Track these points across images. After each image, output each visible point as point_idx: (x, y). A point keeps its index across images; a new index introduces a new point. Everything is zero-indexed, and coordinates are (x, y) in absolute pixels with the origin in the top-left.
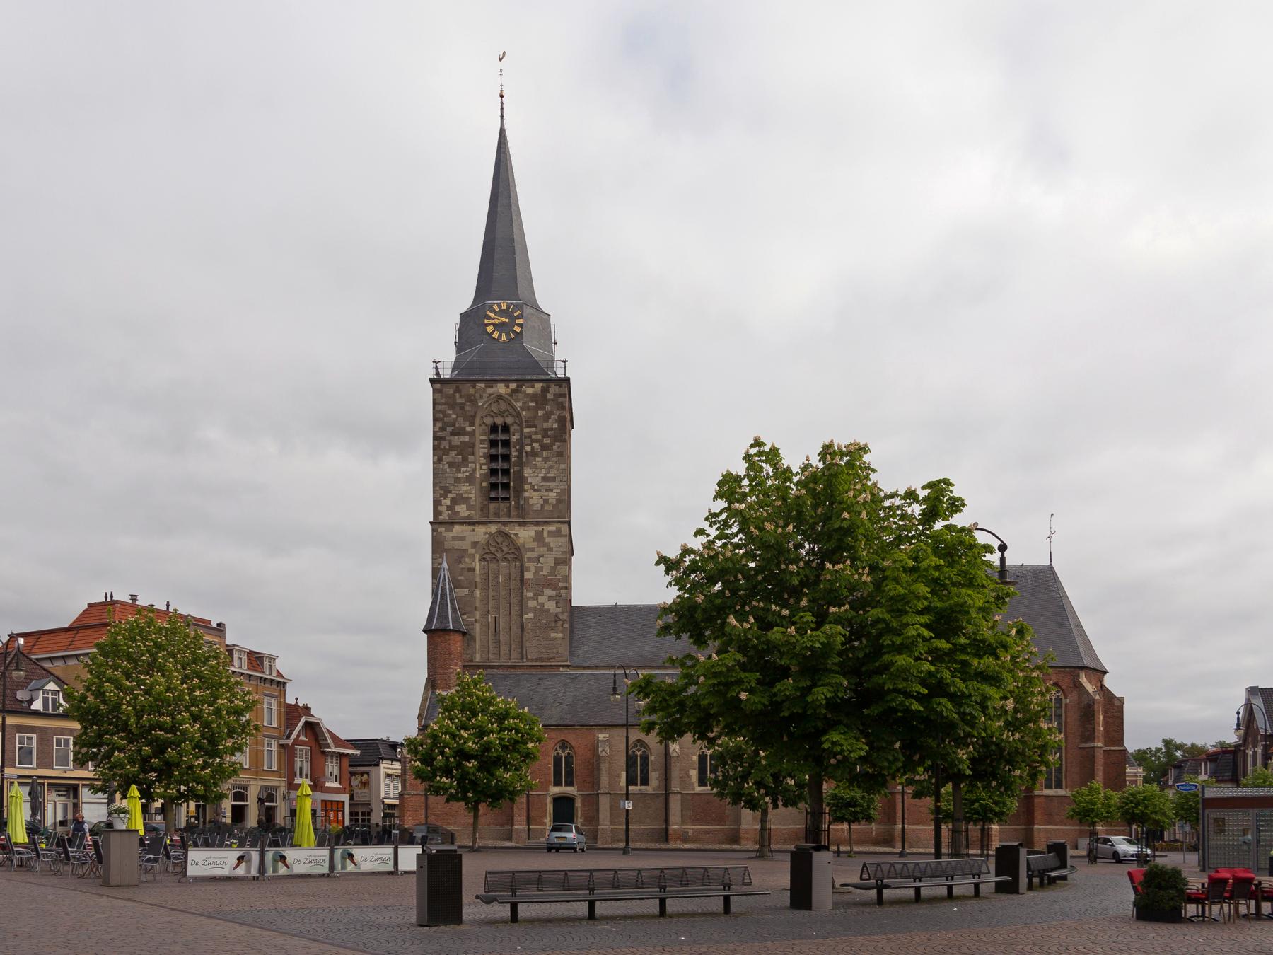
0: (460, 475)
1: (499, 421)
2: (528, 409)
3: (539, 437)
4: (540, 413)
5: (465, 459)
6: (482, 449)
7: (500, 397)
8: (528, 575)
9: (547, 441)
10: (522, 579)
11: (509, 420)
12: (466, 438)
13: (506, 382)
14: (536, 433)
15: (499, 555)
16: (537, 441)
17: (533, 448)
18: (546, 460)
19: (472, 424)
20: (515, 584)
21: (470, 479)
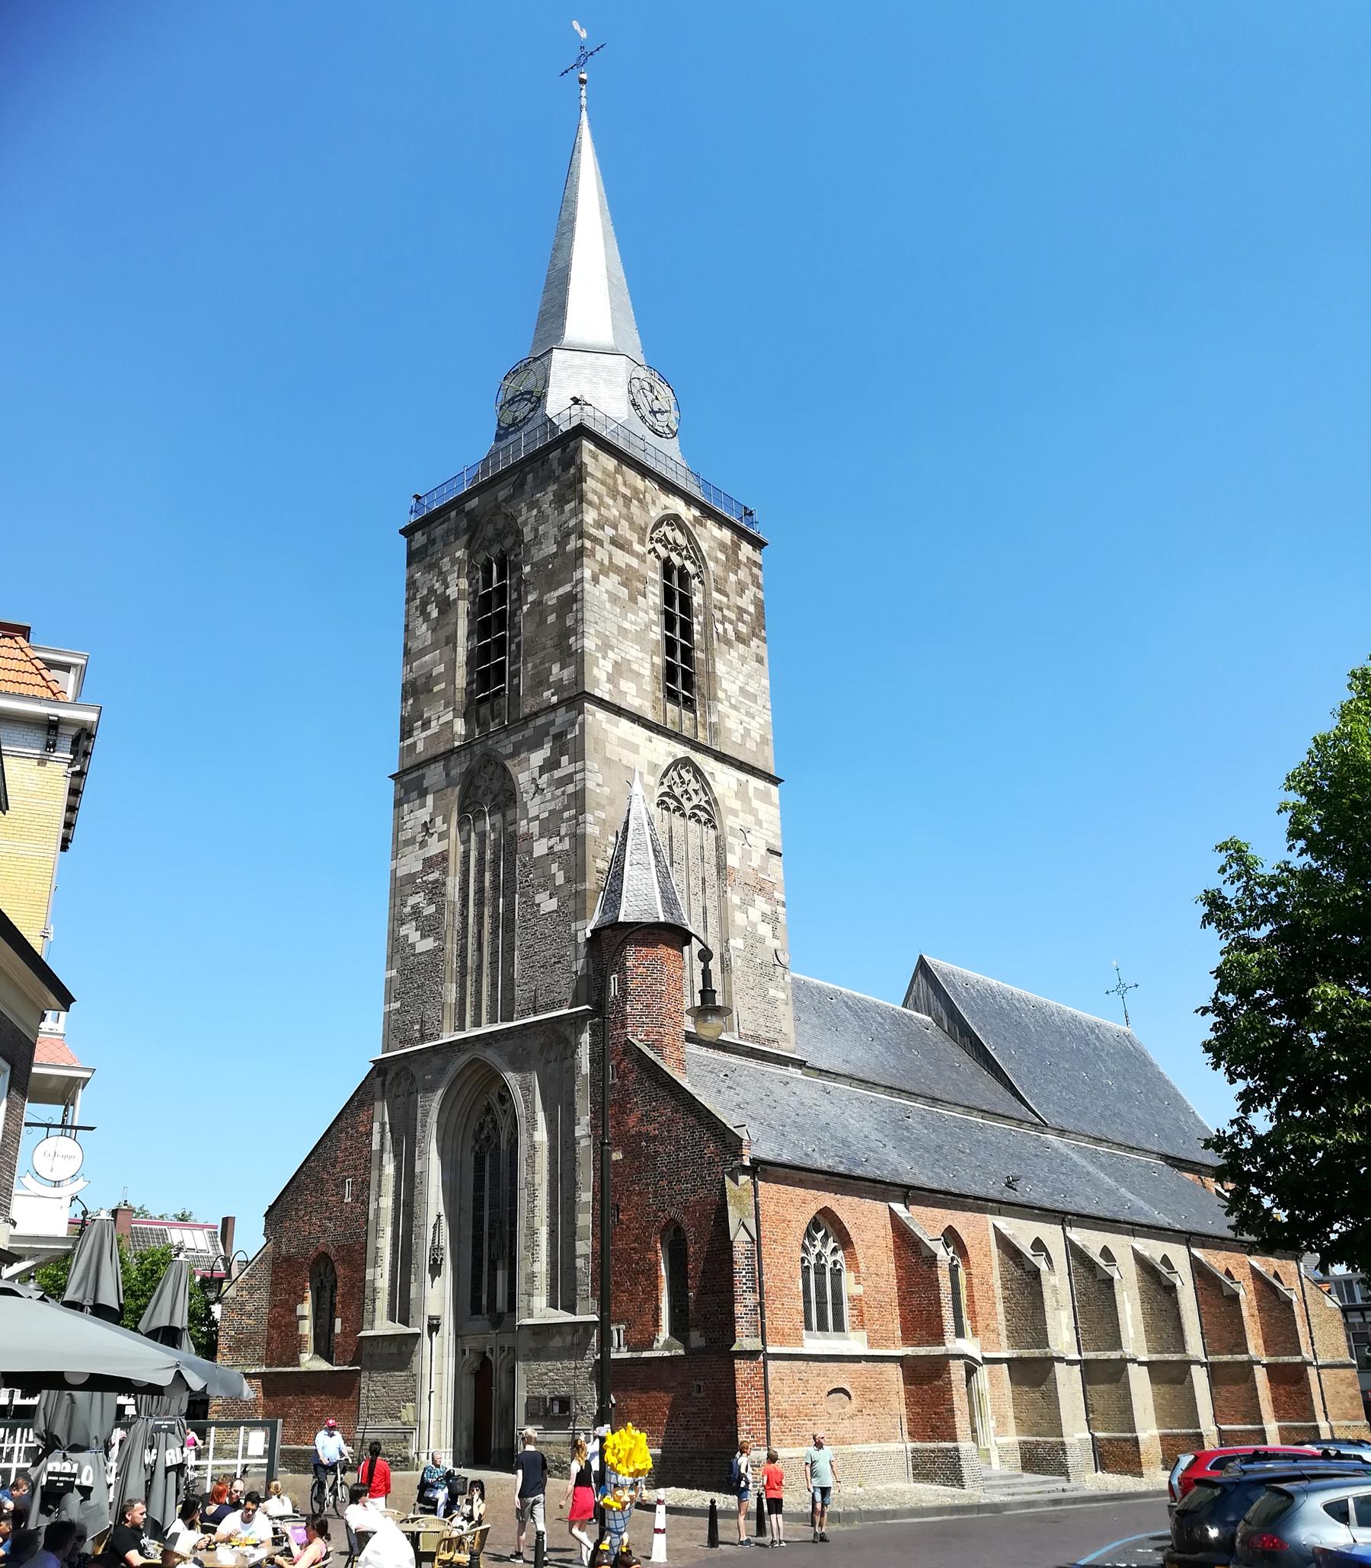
0: (626, 625)
1: (676, 560)
2: (717, 561)
3: (733, 616)
4: (732, 578)
5: (633, 599)
6: (654, 596)
7: (674, 520)
8: (732, 860)
9: (743, 628)
10: (721, 867)
11: (691, 568)
12: (635, 563)
13: (689, 500)
14: (728, 608)
15: (687, 806)
16: (731, 622)
17: (725, 630)
18: (743, 659)
19: (642, 542)
20: (711, 871)
21: (639, 638)
